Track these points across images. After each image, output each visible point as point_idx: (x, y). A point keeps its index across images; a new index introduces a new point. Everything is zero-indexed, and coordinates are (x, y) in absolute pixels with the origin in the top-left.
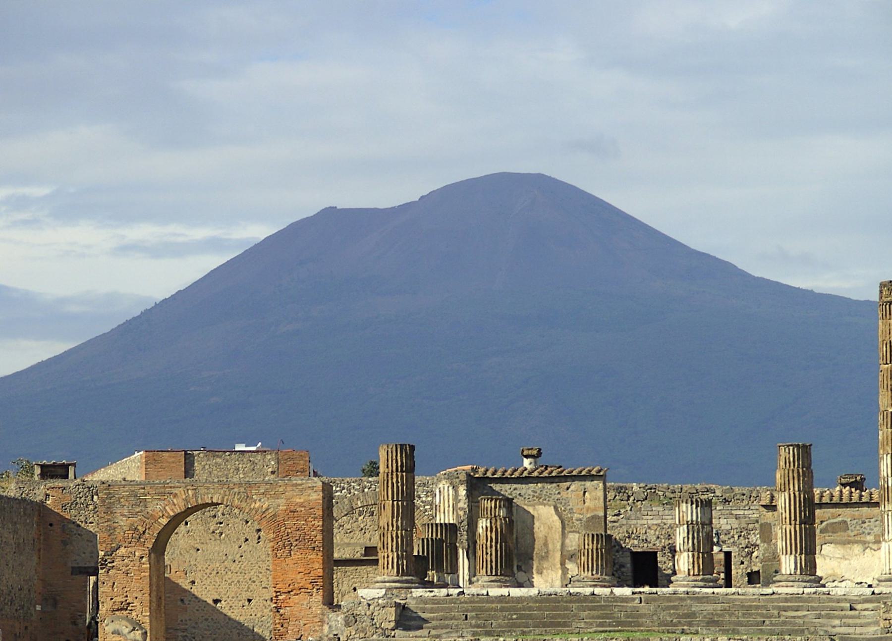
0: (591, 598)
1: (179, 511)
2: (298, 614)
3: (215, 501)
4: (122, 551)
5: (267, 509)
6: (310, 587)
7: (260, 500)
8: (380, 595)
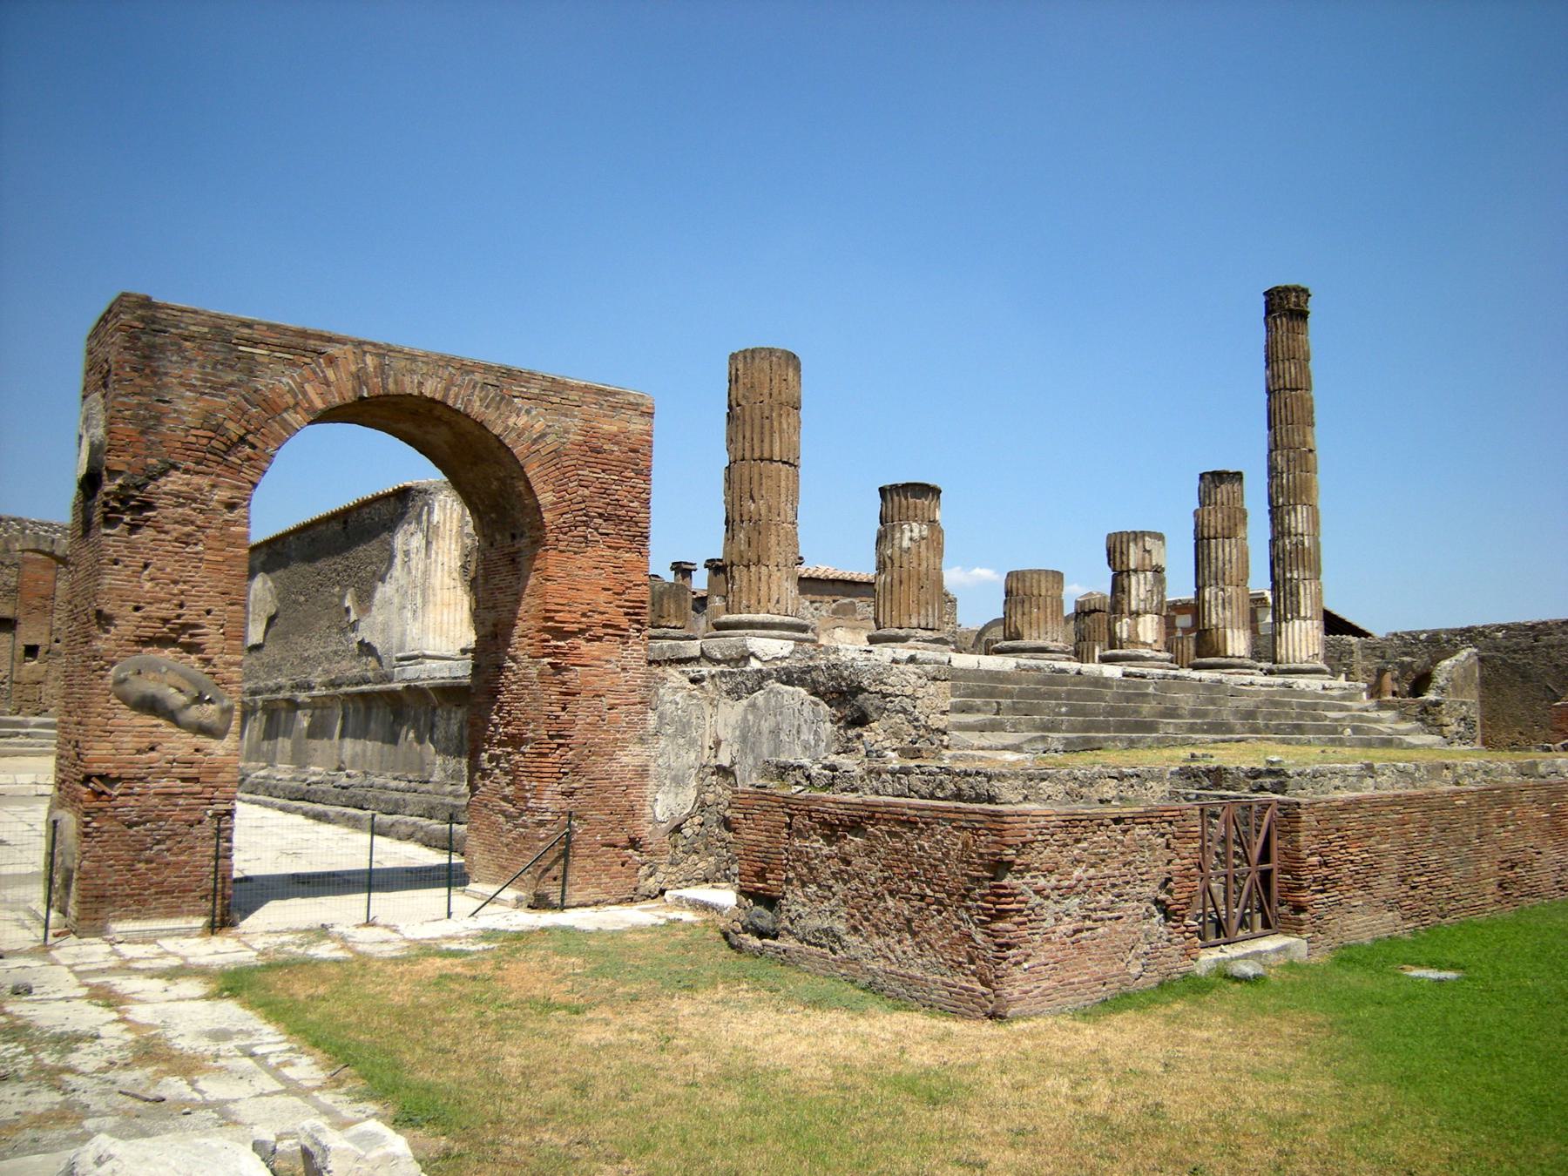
0: (1078, 678)
1: (337, 401)
2: (598, 684)
3: (427, 392)
4: (174, 482)
5: (543, 436)
6: (624, 622)
7: (528, 412)
8: (786, 652)
